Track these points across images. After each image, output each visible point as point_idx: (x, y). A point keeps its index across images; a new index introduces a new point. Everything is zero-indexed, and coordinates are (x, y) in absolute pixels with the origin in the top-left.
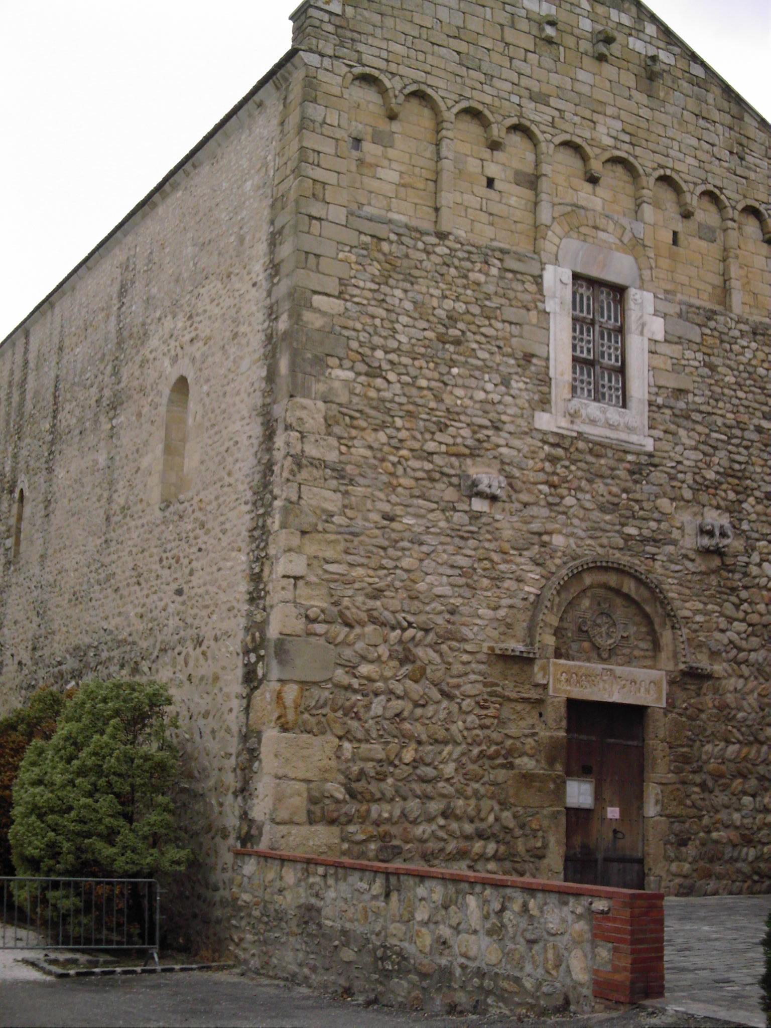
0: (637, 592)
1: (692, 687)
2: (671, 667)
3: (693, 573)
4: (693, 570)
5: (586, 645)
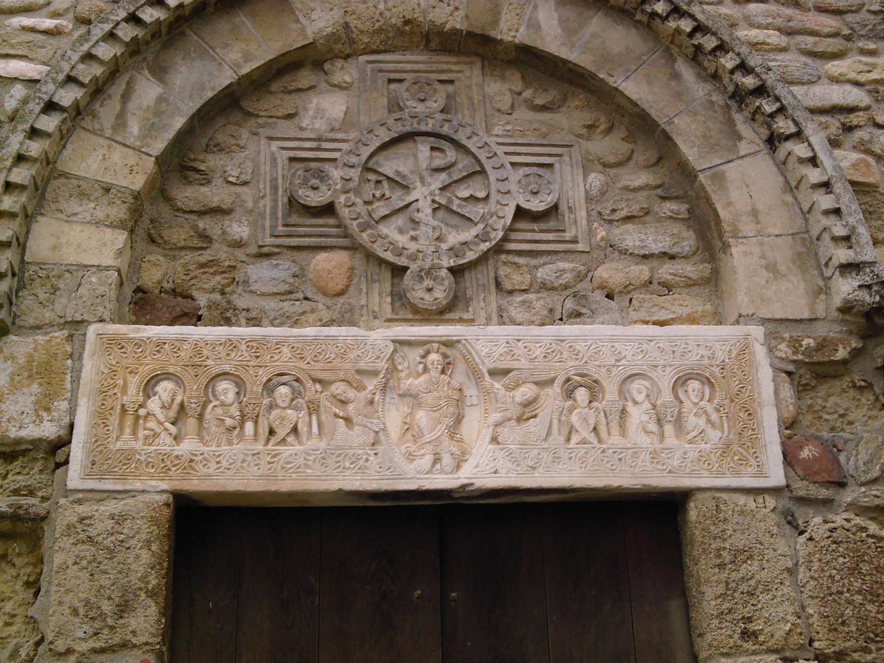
0: (569, 32)
2: (791, 298)
5: (329, 264)
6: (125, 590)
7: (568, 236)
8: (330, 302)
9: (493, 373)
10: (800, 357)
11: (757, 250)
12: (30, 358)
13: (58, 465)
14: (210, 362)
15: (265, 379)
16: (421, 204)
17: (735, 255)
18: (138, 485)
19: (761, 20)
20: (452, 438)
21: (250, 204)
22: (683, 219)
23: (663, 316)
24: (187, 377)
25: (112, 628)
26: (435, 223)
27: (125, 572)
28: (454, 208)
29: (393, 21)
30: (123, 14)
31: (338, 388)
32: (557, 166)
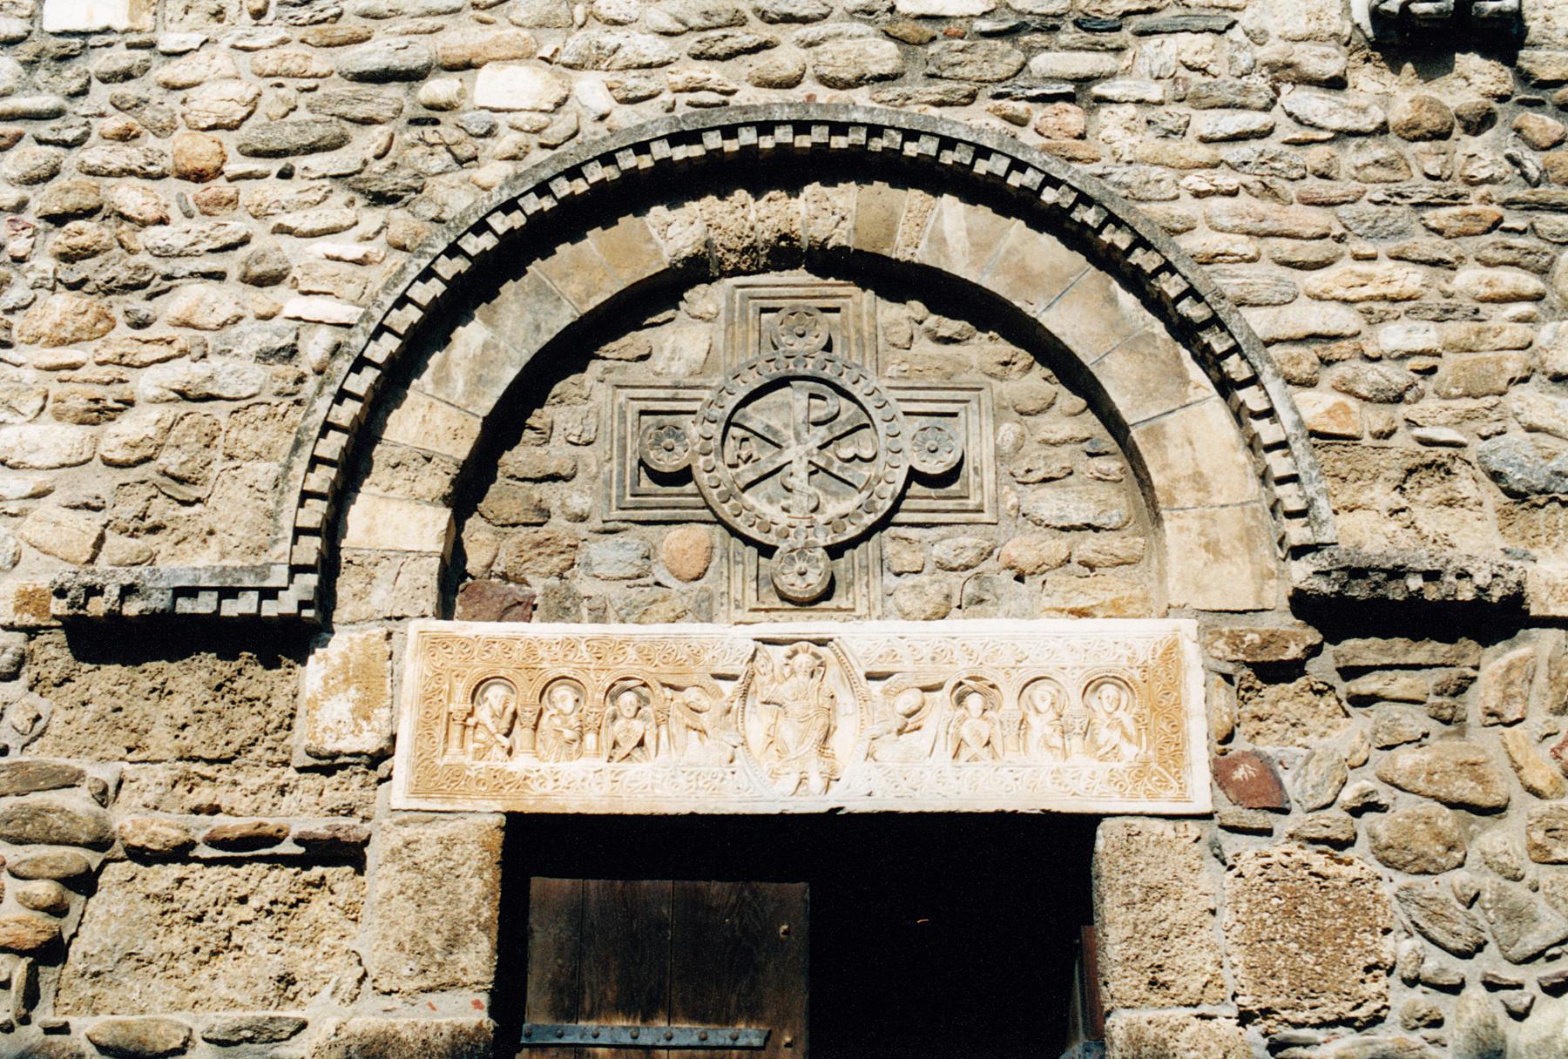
1: (1401, 684)
3: (1342, 135)
4: (1336, 122)
5: (684, 542)
6: (455, 923)
7: (971, 503)
8: (685, 587)
9: (870, 677)
10: (1241, 656)
11: (1195, 526)
12: (346, 659)
13: (381, 781)
14: (545, 665)
15: (608, 685)
16: (793, 467)
17: (1168, 532)
18: (469, 806)
19: (1226, 222)
20: (821, 754)
21: (594, 469)
22: (1114, 481)
23: (1081, 602)
24: (520, 679)
25: (440, 965)
26: (812, 490)
27: (454, 901)
28: (835, 471)
29: (766, 236)
30: (443, 246)
31: (691, 695)
32: (962, 415)
